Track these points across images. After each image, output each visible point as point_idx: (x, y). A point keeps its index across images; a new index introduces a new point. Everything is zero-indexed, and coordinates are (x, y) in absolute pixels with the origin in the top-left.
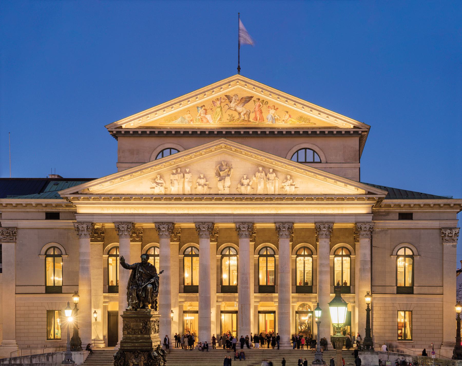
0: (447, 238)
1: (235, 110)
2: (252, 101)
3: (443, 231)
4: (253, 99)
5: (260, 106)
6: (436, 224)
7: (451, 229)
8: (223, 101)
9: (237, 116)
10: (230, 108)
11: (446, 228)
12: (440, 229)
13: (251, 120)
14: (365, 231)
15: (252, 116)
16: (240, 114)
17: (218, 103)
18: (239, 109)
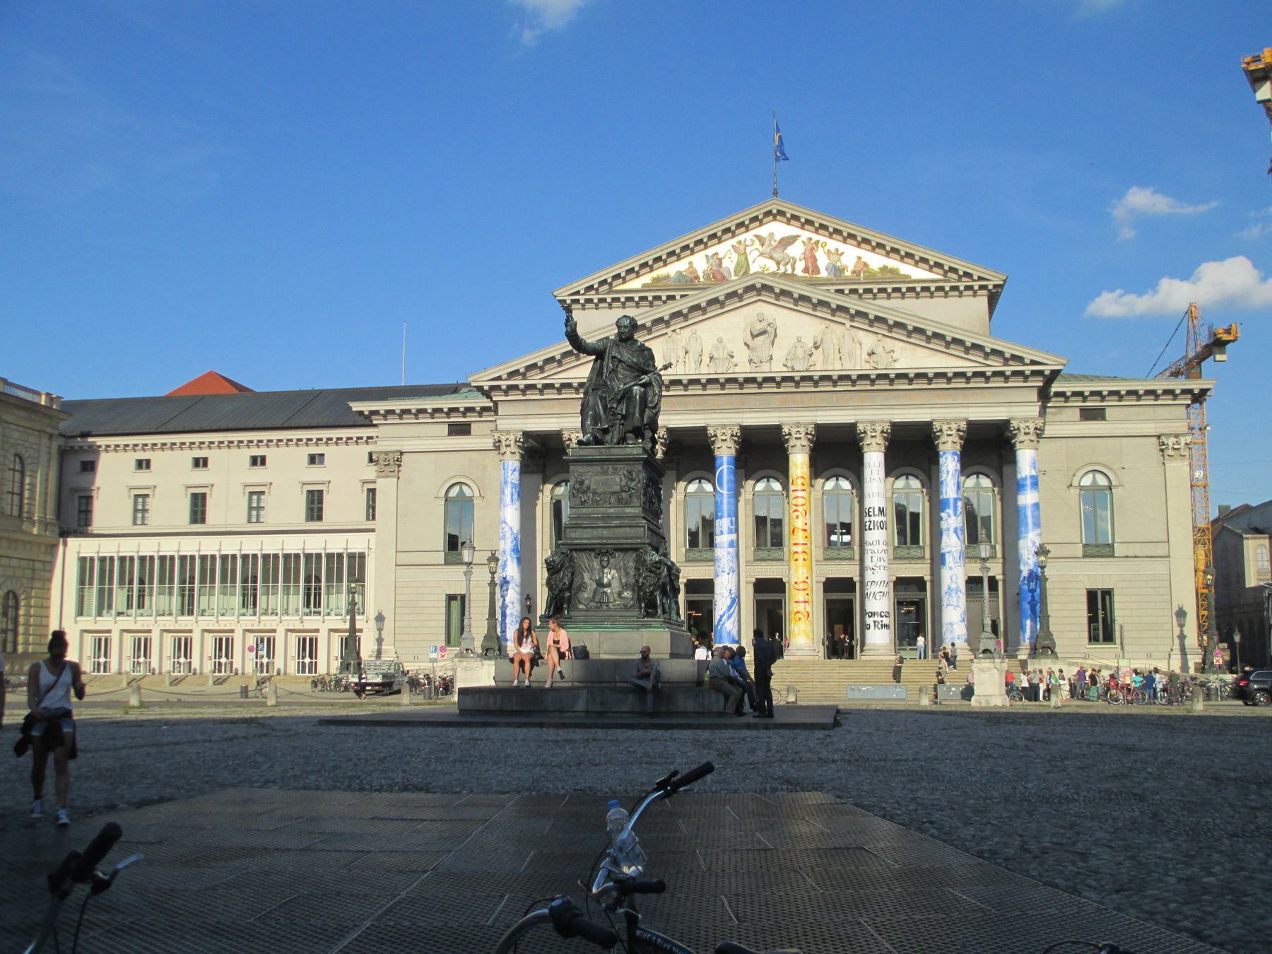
0: (1170, 452)
1: (771, 258)
2: (798, 243)
3: (1163, 439)
4: (800, 240)
5: (812, 249)
6: (1150, 428)
7: (1177, 436)
8: (748, 243)
10: (761, 254)
11: (1168, 435)
12: (1159, 437)
14: (1026, 434)
16: (778, 263)
17: (742, 247)
18: (777, 255)
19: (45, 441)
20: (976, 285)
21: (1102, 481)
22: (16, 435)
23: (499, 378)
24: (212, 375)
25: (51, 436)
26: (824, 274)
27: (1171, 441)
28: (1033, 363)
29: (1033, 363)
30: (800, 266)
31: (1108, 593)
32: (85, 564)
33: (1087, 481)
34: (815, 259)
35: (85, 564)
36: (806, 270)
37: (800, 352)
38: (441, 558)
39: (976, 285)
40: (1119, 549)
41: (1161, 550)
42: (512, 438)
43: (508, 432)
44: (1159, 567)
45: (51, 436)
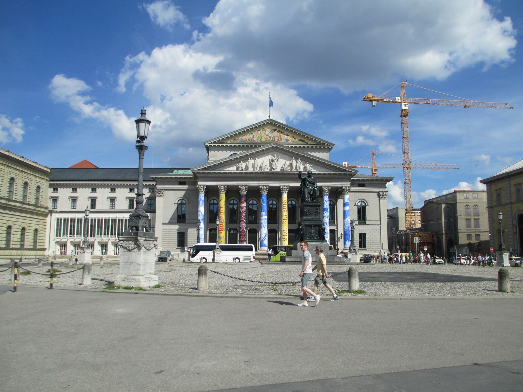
9: (269, 138)
13: (276, 140)
15: (276, 138)
18: (270, 135)
20: (326, 147)
21: (363, 204)
23: (200, 170)
24: (85, 161)
26: (283, 141)
27: (382, 193)
28: (349, 171)
29: (349, 171)
30: (276, 138)
31: (364, 235)
32: (59, 221)
33: (359, 204)
34: (281, 137)
35: (59, 221)
36: (278, 140)
37: (286, 166)
38: (176, 221)
39: (326, 147)
40: (368, 223)
41: (378, 223)
42: (202, 187)
43: (201, 185)
44: (379, 228)
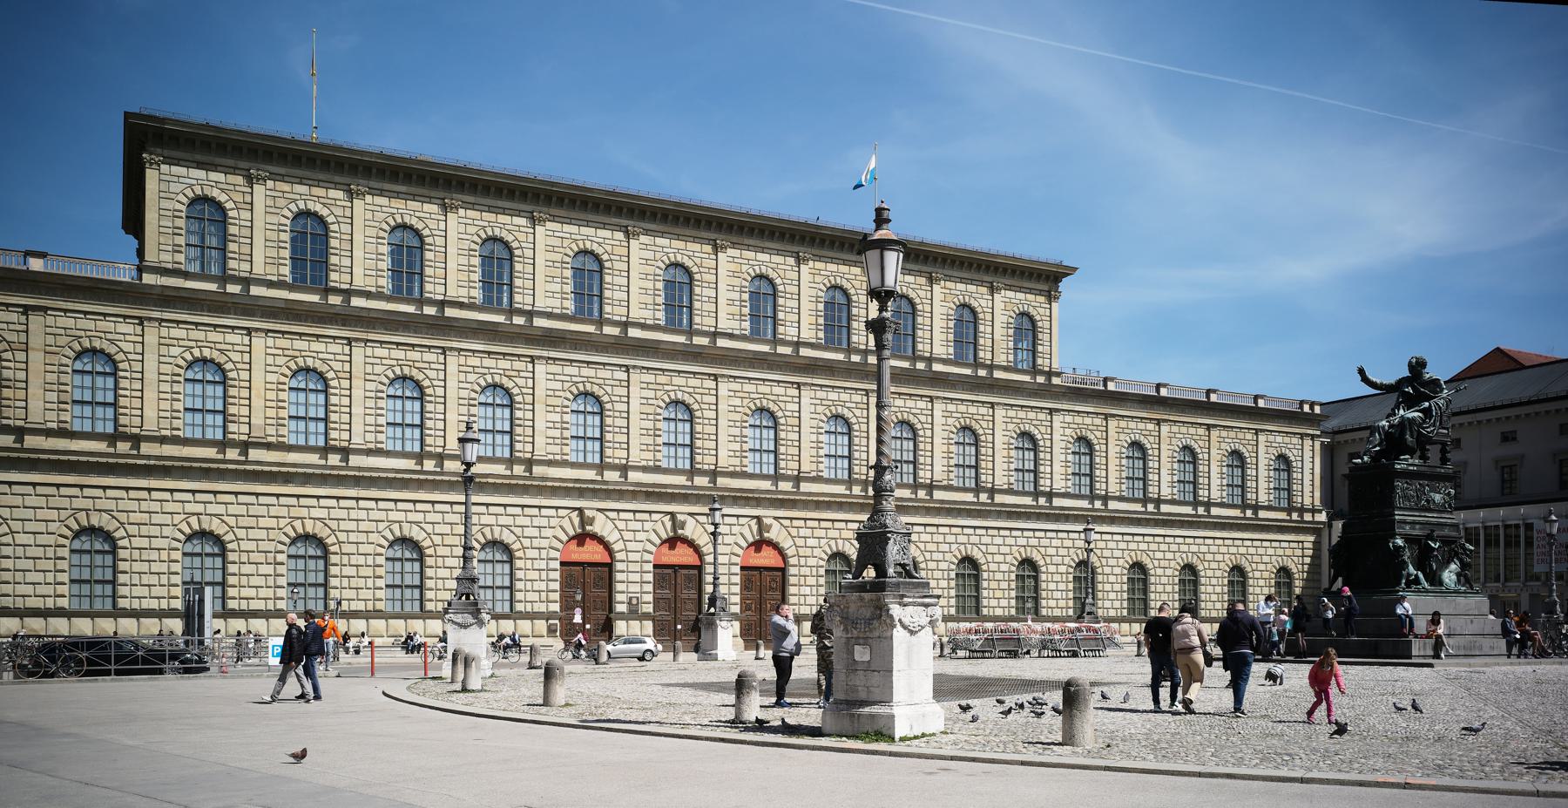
19: (1308, 442)
22: (1279, 439)
25: (1313, 437)
45: (1313, 437)
